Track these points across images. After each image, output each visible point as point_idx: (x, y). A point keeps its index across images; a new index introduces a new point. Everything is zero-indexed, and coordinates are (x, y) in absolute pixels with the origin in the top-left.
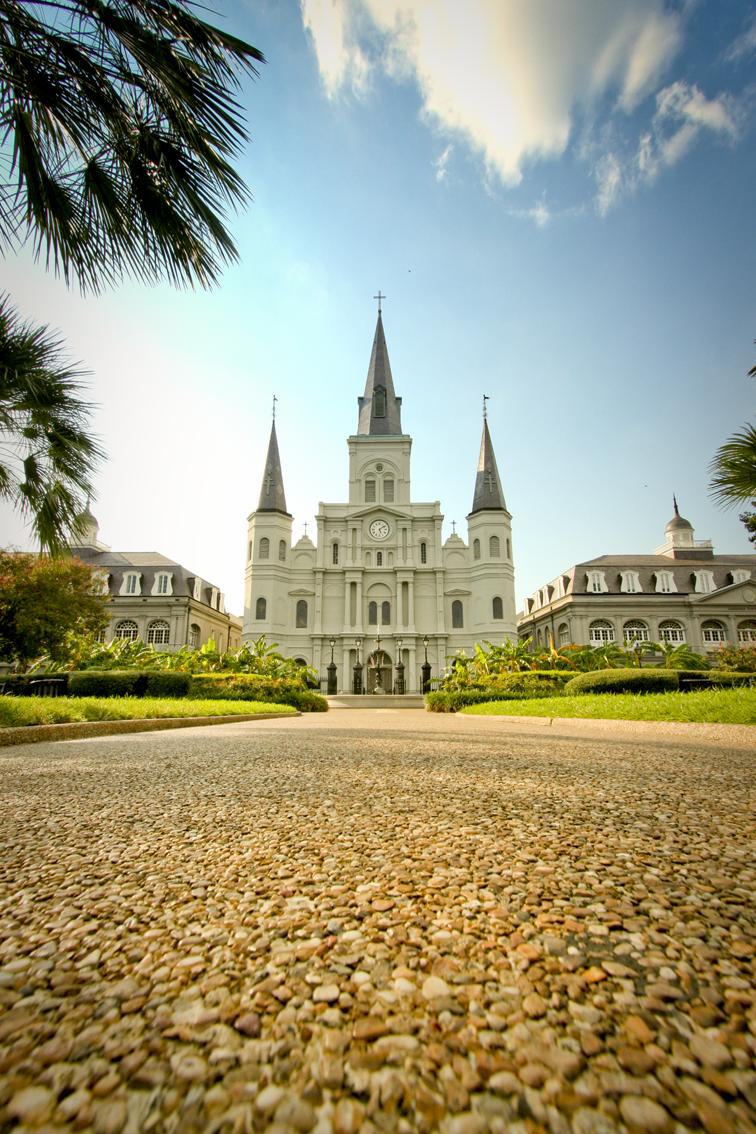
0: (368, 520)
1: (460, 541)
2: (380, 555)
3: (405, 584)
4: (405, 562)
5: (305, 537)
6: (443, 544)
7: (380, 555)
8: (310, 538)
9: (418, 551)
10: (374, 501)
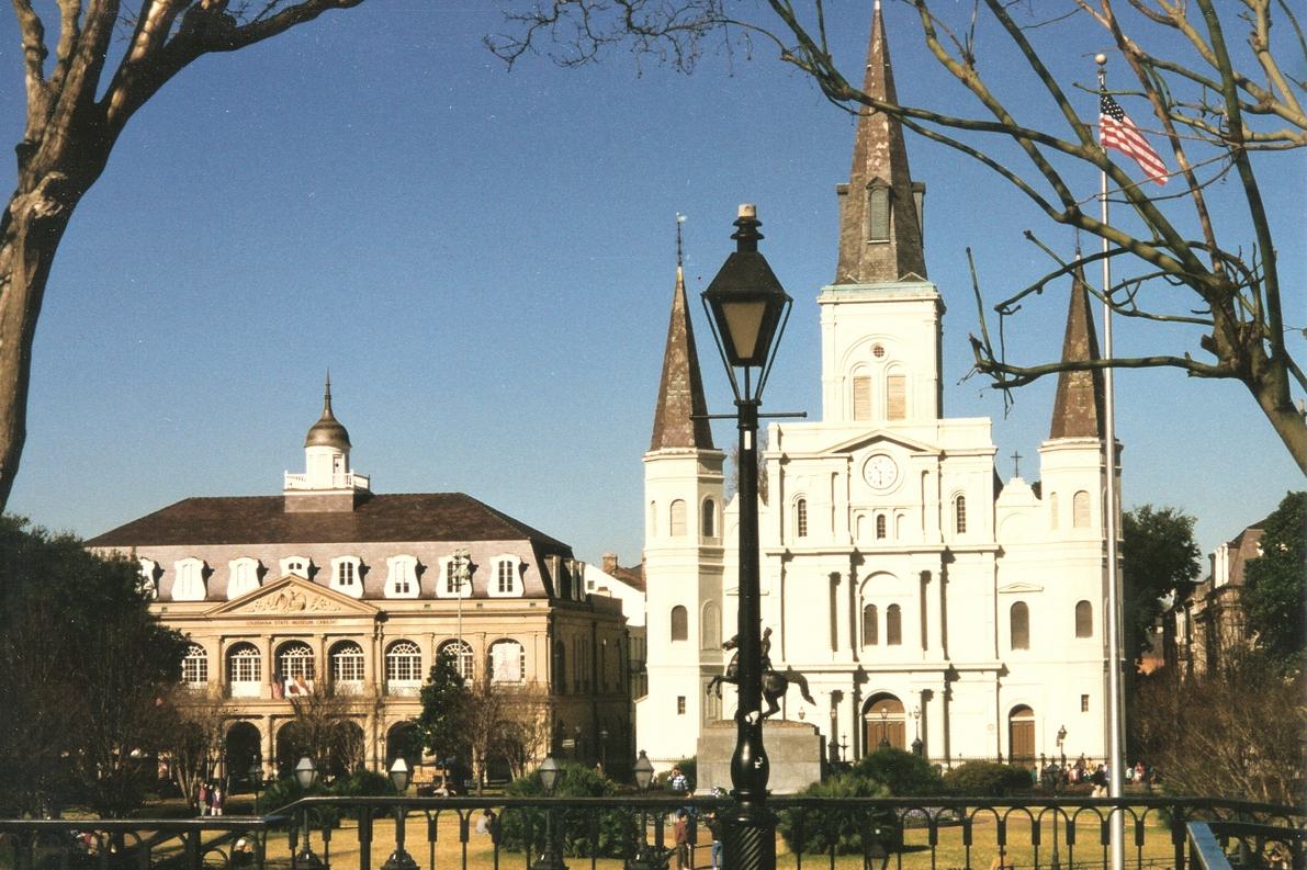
2: (881, 518)
7: (881, 518)
9: (950, 513)
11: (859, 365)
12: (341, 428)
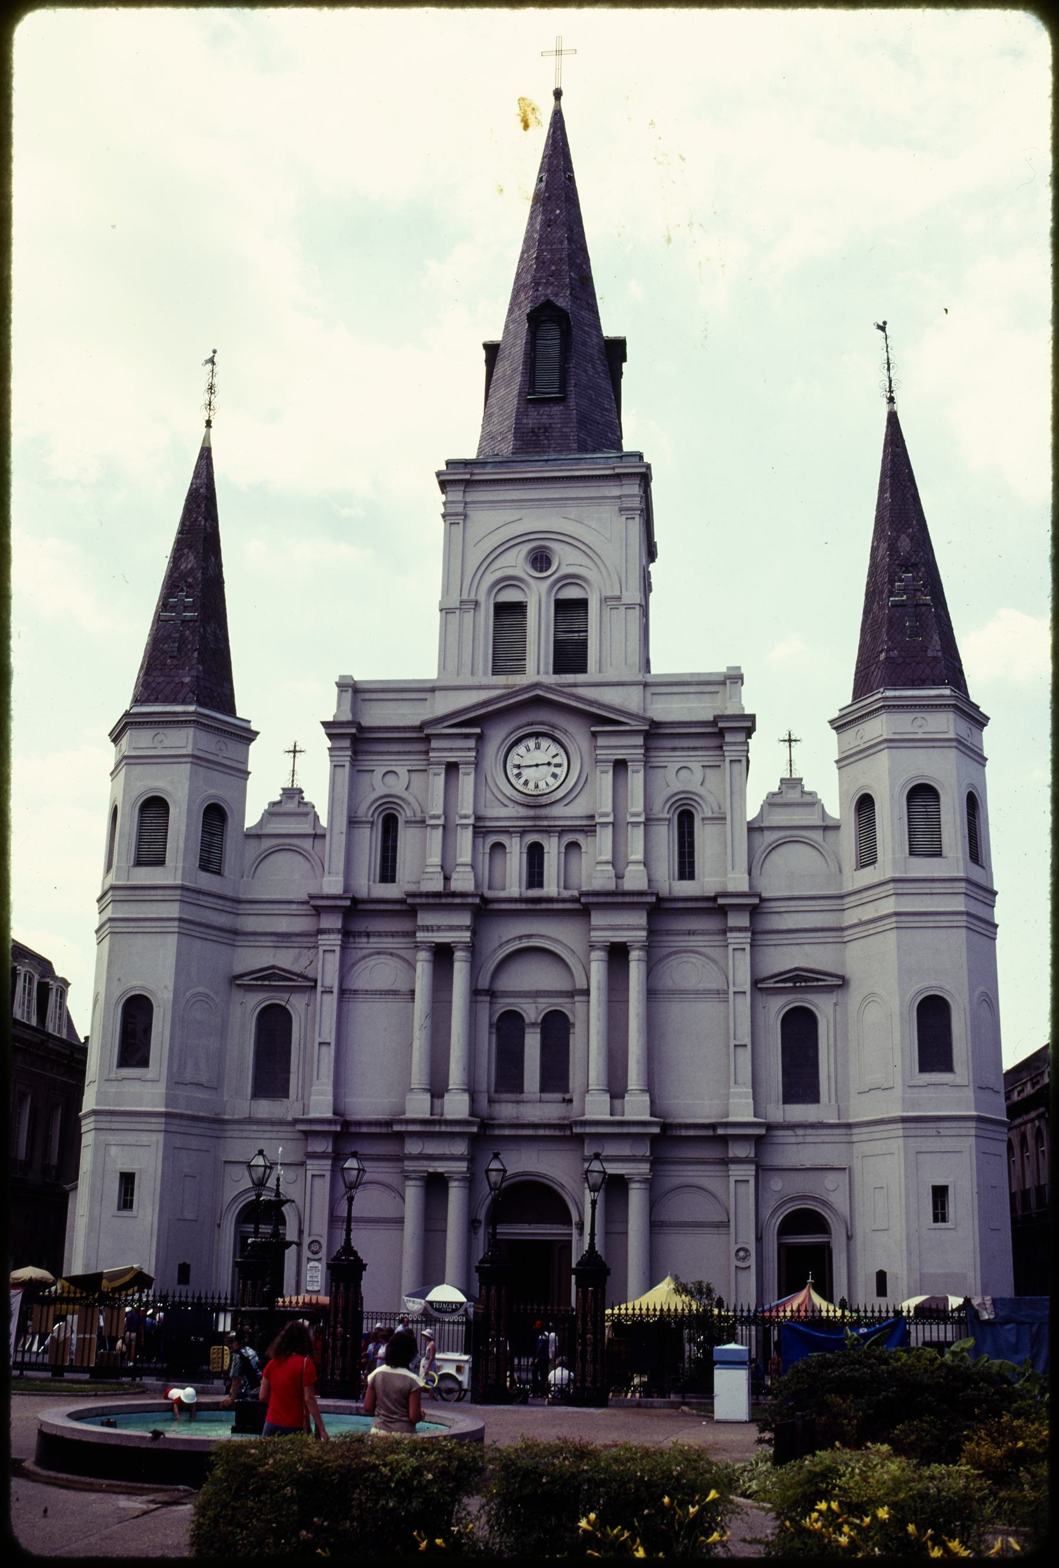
0: (498, 736)
1: (811, 802)
3: (618, 954)
5: (292, 793)
6: (752, 811)
8: (307, 797)
9: (666, 838)
10: (521, 670)
11: (509, 582)
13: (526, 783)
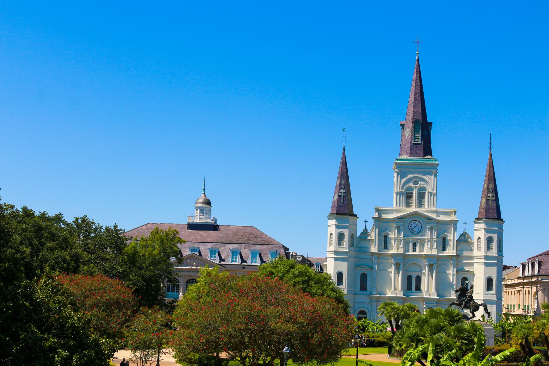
4: (431, 250)
10: (412, 206)
12: (209, 200)
13: (413, 230)
